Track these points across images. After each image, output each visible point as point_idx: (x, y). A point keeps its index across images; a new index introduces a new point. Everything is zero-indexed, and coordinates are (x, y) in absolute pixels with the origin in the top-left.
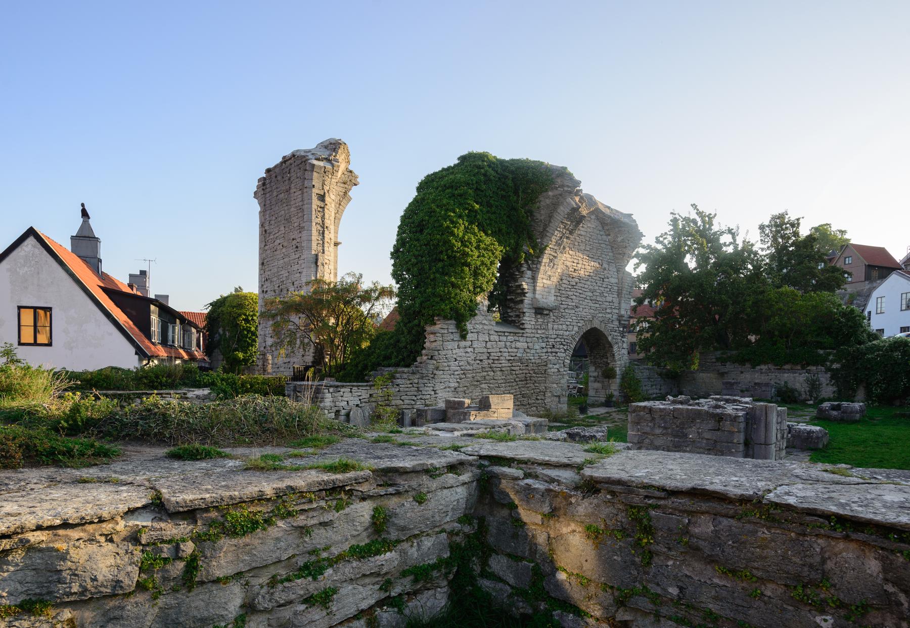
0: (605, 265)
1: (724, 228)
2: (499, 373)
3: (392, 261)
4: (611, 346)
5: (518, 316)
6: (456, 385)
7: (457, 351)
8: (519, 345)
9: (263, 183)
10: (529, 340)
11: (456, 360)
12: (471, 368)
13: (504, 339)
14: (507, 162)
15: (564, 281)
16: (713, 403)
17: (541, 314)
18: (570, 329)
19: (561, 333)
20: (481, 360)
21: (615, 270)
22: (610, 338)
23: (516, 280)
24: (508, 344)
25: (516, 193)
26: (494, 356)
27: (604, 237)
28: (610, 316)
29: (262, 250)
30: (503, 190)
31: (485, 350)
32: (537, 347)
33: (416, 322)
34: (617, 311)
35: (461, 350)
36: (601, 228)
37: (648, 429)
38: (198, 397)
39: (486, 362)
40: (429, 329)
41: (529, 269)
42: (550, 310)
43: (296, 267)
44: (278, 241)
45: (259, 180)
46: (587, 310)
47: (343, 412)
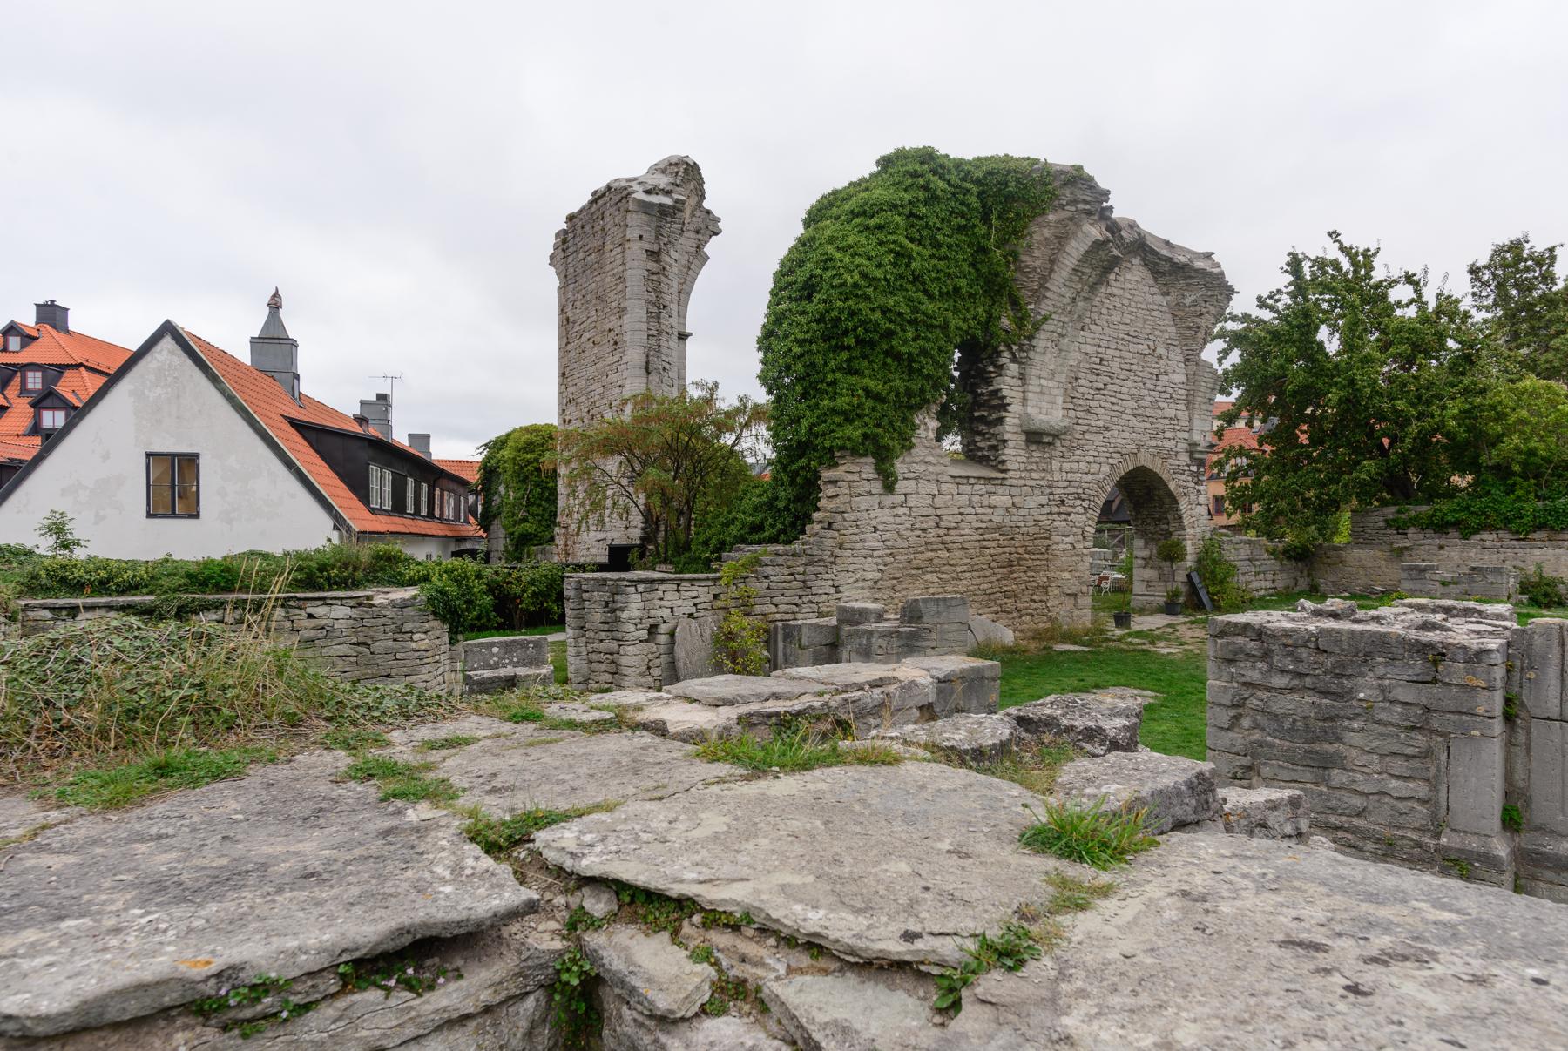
1: (1396, 273)
2: (959, 554)
3: (761, 355)
4: (1174, 501)
5: (994, 448)
6: (877, 575)
7: (878, 512)
8: (994, 500)
9: (565, 242)
10: (1014, 491)
11: (876, 529)
12: (905, 544)
13: (966, 489)
14: (970, 163)
15: (1082, 382)
16: (1418, 617)
17: (1039, 443)
18: (1093, 470)
19: (1077, 477)
20: (924, 530)
21: (1180, 358)
22: (1172, 486)
23: (989, 382)
24: (976, 499)
25: (986, 219)
26: (948, 521)
27: (1159, 298)
28: (1171, 444)
29: (563, 351)
30: (963, 215)
31: (931, 511)
32: (1031, 503)
33: (803, 462)
34: (1186, 435)
35: (886, 511)
36: (1151, 282)
37: (1254, 676)
38: (393, 604)
39: (933, 532)
40: (826, 474)
41: (1014, 360)
42: (1056, 436)
43: (614, 378)
44: (587, 335)
45: (557, 235)
46: (1125, 434)
47: (663, 628)
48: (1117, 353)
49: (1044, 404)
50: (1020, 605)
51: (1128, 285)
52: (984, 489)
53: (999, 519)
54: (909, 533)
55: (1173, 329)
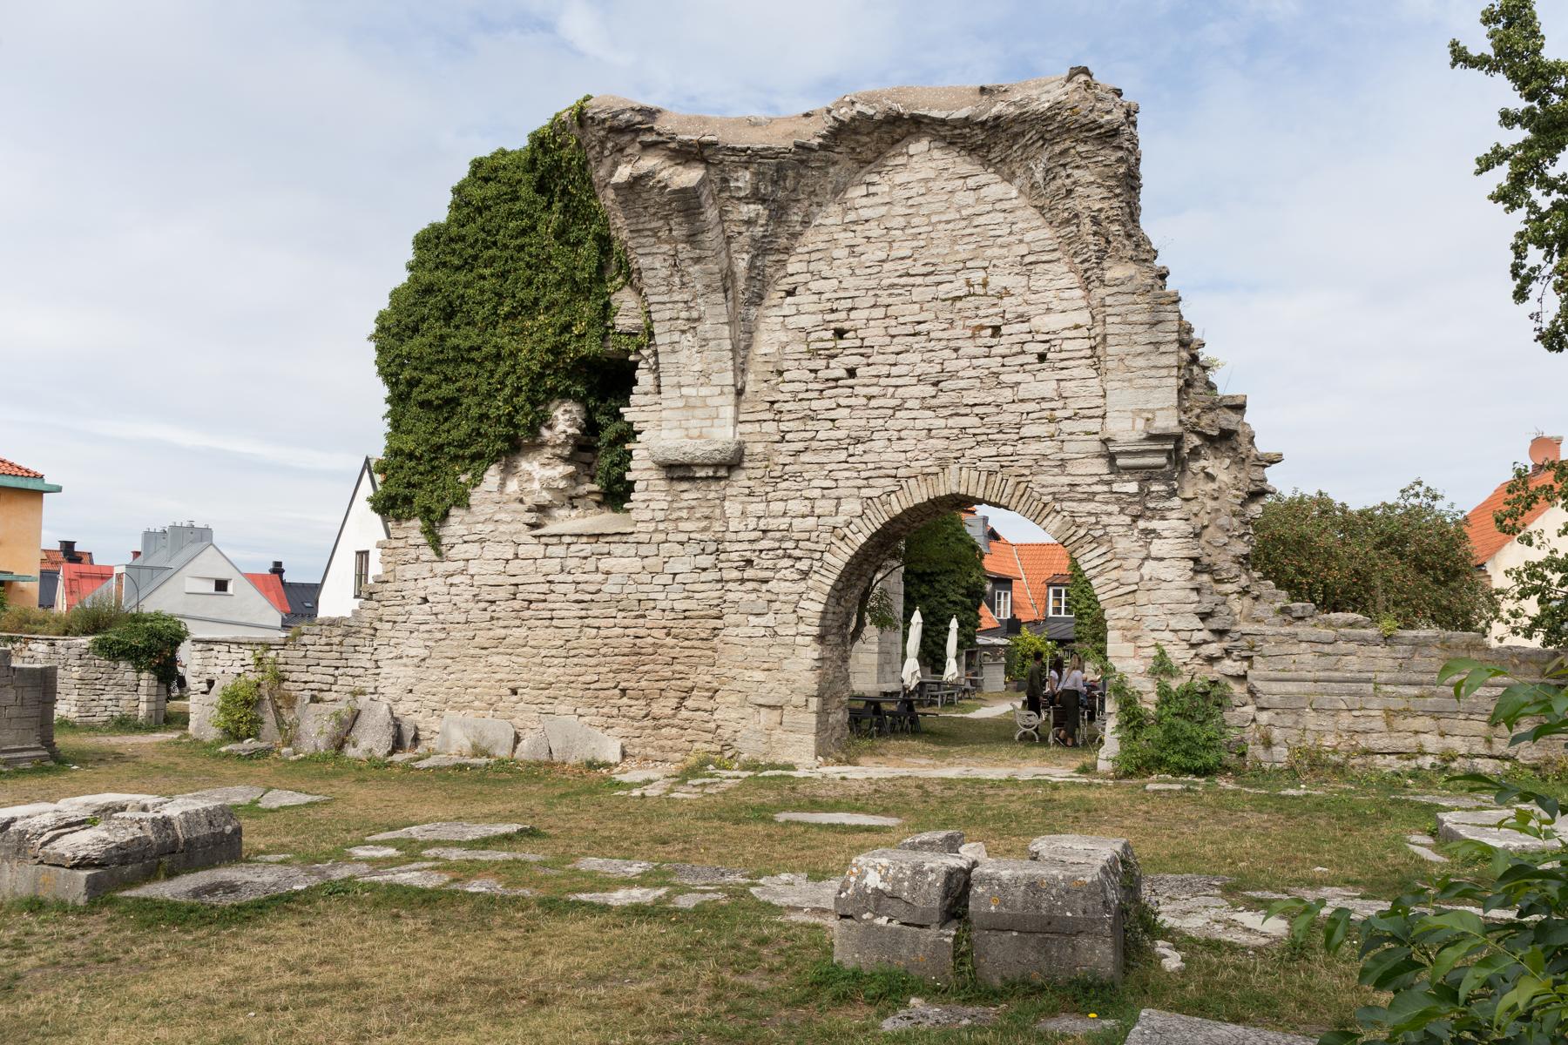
0: (997, 281)
6: (424, 653)
8: (605, 564)
10: (643, 550)
11: (425, 600)
13: (559, 550)
19: (783, 523)
20: (493, 602)
21: (1074, 279)
28: (1047, 447)
34: (1094, 425)
48: (880, 312)
49: (693, 423)
50: (656, 709)
51: (900, 194)
52: (588, 549)
53: (616, 589)
54: (471, 605)
55: (1047, 233)
